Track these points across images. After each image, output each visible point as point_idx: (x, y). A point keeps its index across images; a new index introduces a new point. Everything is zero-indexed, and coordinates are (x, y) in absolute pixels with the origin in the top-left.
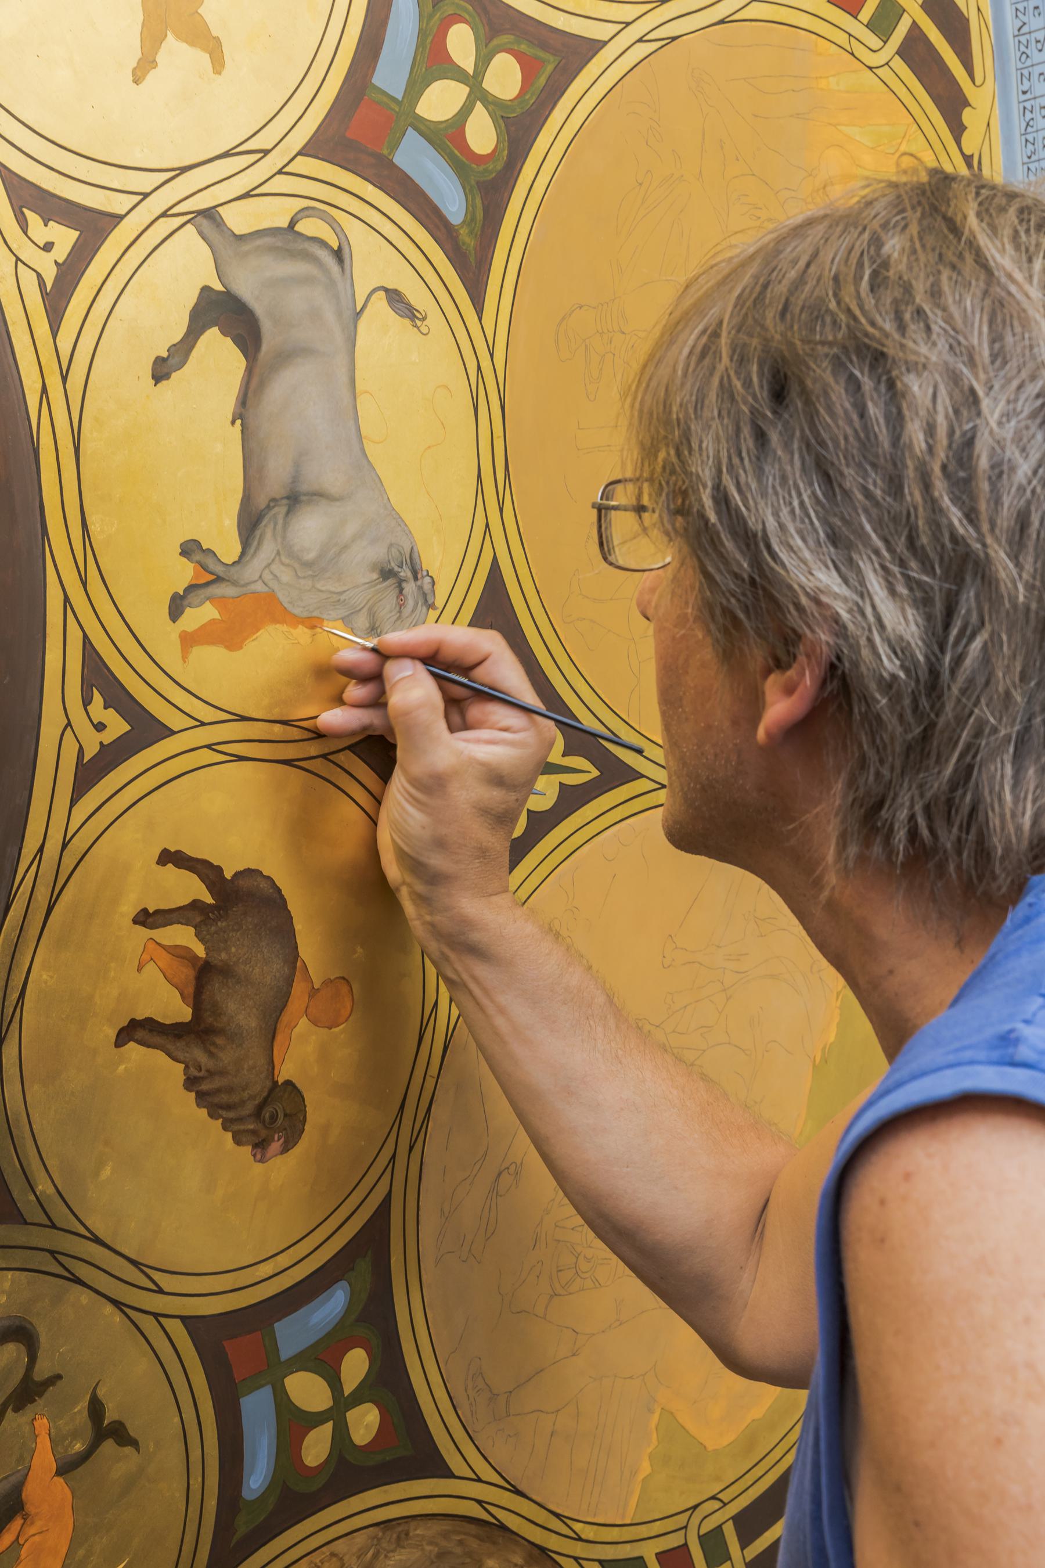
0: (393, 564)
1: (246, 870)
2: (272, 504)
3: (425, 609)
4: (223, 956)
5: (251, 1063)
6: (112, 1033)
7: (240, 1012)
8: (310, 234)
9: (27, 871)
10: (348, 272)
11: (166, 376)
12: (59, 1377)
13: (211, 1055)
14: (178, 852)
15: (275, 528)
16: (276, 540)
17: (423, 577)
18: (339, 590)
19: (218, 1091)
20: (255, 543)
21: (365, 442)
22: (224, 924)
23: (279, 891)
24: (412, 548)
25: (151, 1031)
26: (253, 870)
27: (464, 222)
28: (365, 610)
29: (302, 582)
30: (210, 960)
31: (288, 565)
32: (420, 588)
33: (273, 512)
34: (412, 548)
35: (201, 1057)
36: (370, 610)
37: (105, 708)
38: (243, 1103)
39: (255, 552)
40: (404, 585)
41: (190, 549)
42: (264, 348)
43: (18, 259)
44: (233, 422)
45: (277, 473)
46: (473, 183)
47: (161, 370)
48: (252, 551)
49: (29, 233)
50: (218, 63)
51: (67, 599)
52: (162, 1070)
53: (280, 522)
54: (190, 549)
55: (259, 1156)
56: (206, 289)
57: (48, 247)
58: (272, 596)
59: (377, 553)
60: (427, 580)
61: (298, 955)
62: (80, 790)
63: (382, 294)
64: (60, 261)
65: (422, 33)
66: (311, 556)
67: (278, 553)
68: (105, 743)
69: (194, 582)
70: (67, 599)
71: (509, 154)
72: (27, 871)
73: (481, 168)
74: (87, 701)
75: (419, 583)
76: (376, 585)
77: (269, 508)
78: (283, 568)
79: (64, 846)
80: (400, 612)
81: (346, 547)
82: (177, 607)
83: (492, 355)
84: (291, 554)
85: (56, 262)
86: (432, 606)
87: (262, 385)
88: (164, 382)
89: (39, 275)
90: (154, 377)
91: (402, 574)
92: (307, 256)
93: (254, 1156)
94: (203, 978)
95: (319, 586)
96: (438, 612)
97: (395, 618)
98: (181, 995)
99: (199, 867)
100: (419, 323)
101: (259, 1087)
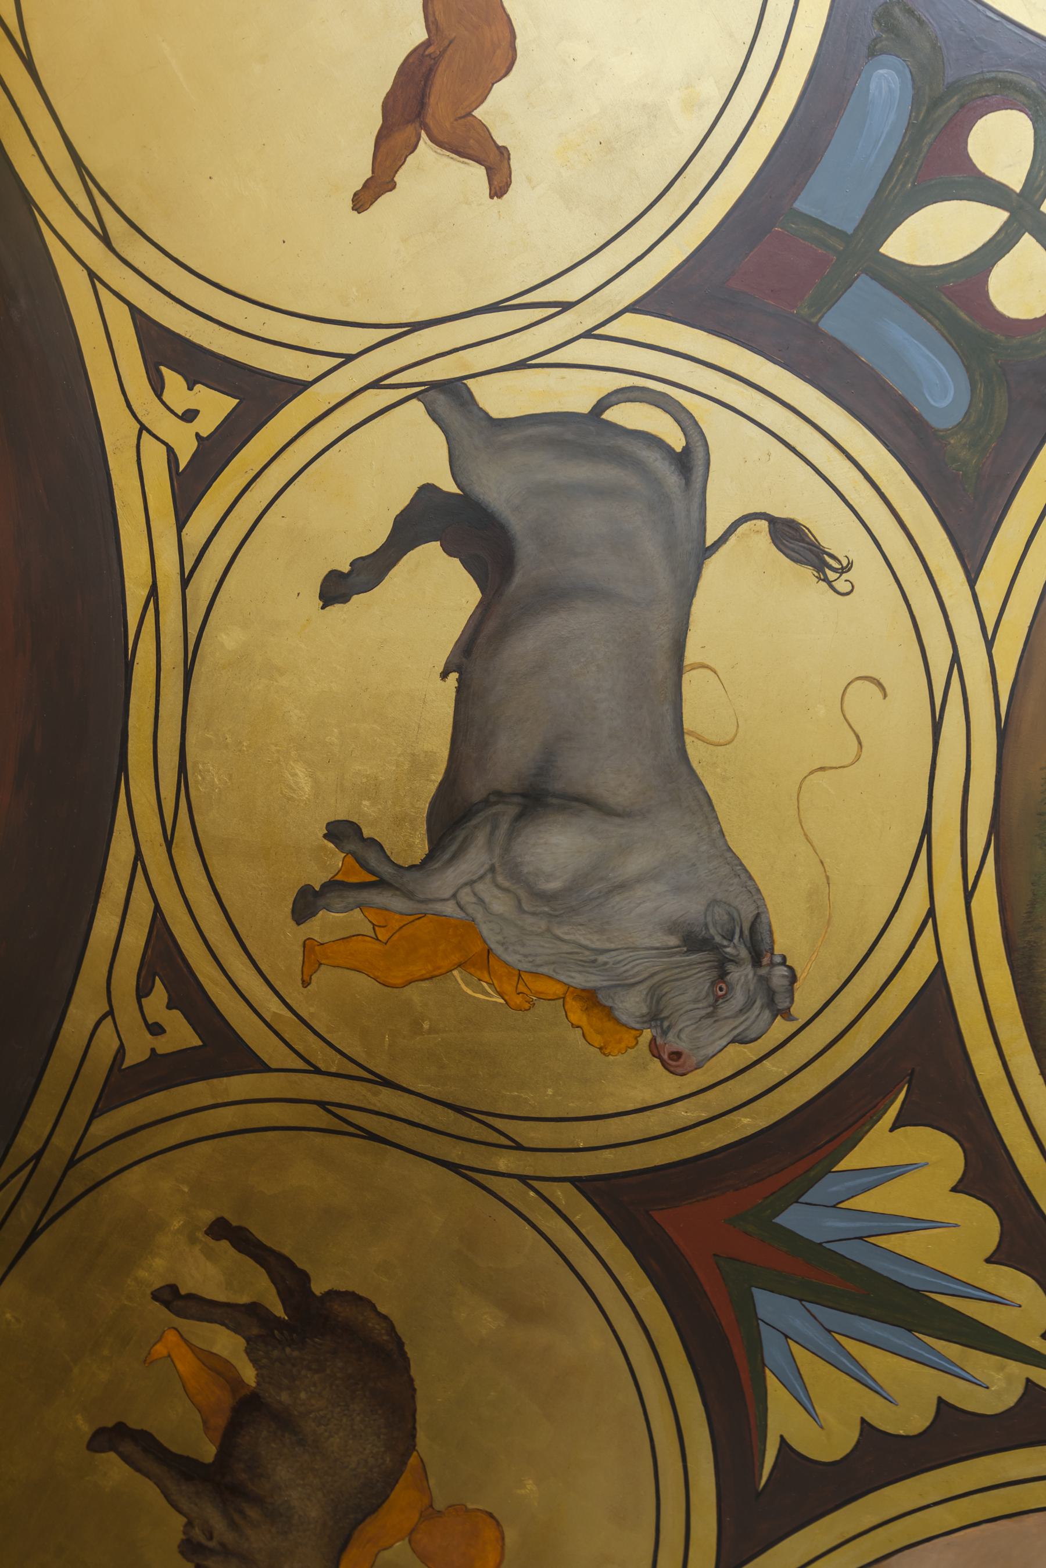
0: (712, 931)
1: (347, 1293)
2: (493, 799)
3: (767, 1014)
4: (284, 1397)
6: (86, 1429)
7: (296, 1485)
8: (630, 425)
9: (13, 1175)
10: (697, 486)
11: (345, 599)
13: (233, 1525)
14: (241, 1229)
15: (492, 833)
17: (772, 965)
18: (598, 945)
20: (454, 848)
21: (688, 739)
22: (296, 1353)
23: (400, 1344)
24: (758, 916)
26: (361, 1298)
27: (960, 426)
28: (643, 988)
32: (764, 981)
33: (494, 809)
34: (758, 916)
35: (218, 1524)
36: (653, 989)
37: (169, 1007)
40: (730, 967)
42: (517, 579)
43: (143, 428)
44: (444, 675)
45: (511, 756)
47: (336, 589)
48: (446, 856)
49: (165, 397)
51: (138, 856)
53: (504, 826)
56: (427, 491)
57: (190, 416)
58: (470, 925)
59: (690, 907)
60: (782, 971)
61: (413, 1447)
63: (764, 524)
64: (204, 434)
65: (915, 133)
66: (554, 885)
67: (492, 869)
69: (339, 878)
70: (138, 856)
72: (13, 1175)
75: (763, 971)
77: (486, 803)
78: (496, 891)
79: (72, 1163)
80: (715, 1006)
81: (623, 887)
82: (306, 903)
83: (989, 644)
84: (515, 873)
85: (197, 435)
86: (786, 1014)
87: (504, 632)
88: (337, 607)
89: (170, 450)
90: (321, 598)
91: (728, 950)
95: (558, 932)
97: (703, 1012)
98: (205, 1422)
100: (831, 575)
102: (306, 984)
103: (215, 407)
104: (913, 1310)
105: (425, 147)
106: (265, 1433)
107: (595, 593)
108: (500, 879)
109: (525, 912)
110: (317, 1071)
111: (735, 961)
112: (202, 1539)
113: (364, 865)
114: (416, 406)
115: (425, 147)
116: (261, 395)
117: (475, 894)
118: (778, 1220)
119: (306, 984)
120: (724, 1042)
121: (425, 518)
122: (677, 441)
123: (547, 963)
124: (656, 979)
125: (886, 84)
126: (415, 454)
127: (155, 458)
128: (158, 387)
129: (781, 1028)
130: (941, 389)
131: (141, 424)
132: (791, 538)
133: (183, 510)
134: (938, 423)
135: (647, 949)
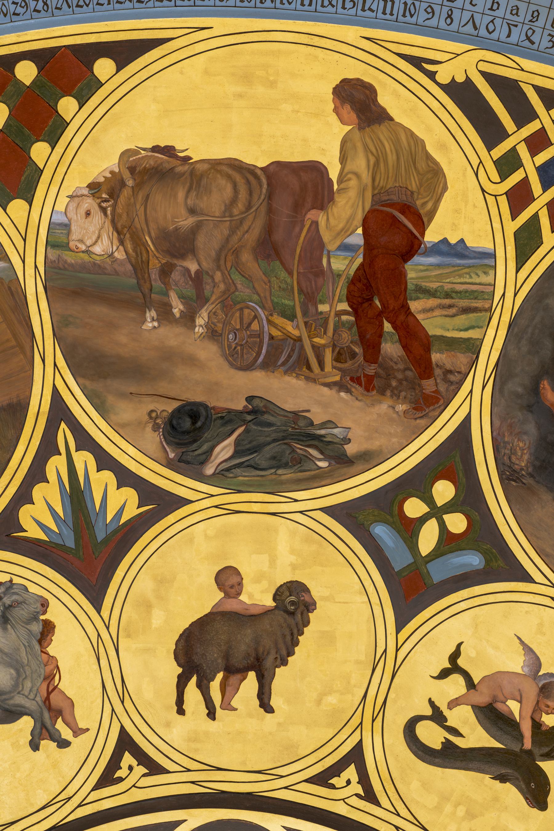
1: (176, 660)
3: (14, 587)
4: (220, 661)
5: (268, 627)
6: (269, 715)
12: (430, 700)
13: (268, 653)
15: (7, 699)
16: (13, 697)
18: (23, 648)
19: (285, 643)
20: (19, 709)
22: (204, 665)
25: (263, 694)
28: (28, 627)
29: (28, 673)
30: (223, 668)
31: (23, 685)
35: (271, 658)
36: (27, 624)
37: (121, 768)
38: (289, 626)
39: (23, 707)
40: (7, 605)
41: (35, 746)
48: (23, 709)
51: (80, 806)
52: (282, 678)
54: (35, 746)
55: (313, 607)
62: (162, 771)
66: (13, 671)
67: (19, 693)
68: (137, 763)
69: (49, 738)
70: (80, 806)
74: (121, 780)
76: (13, 624)
78: (25, 688)
80: (21, 603)
82: (63, 744)
84: (16, 685)
86: (11, 581)
93: (313, 610)
94: (234, 671)
95: (26, 662)
96: (13, 576)
97: (25, 605)
99: (180, 690)
101: (280, 616)
102: (88, 730)
104: (76, 494)
106: (235, 660)
108: (20, 689)
109: (26, 676)
110: (113, 710)
111: (4, 605)
112: (279, 660)
113: (41, 734)
117: (29, 694)
118: (74, 548)
119: (88, 730)
120: (30, 594)
123: (38, 660)
124: (23, 625)
129: (16, 580)
135: (16, 633)
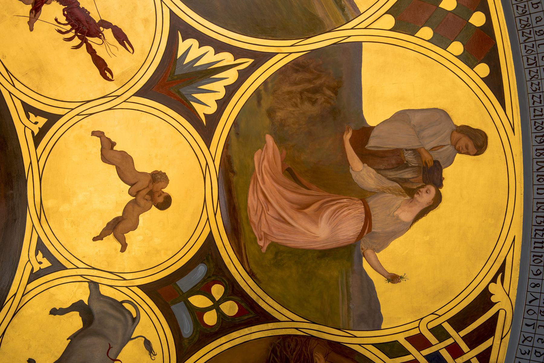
11: (55, 315)
42: (91, 327)
44: (68, 339)
46: (198, 329)
47: (54, 312)
50: (123, 250)
56: (81, 302)
63: (144, 339)
64: (42, 268)
65: (204, 280)
71: (219, 331)
73: (204, 328)
87: (84, 336)
89: (33, 268)
92: (122, 313)
100: (152, 355)
103: (46, 264)
105: (112, 235)
107: (105, 337)
114: (87, 284)
115: (112, 235)
116: (57, 266)
121: (78, 306)
122: (134, 315)
125: (201, 270)
126: (82, 294)
127: (29, 268)
128: (36, 254)
130: (187, 330)
131: (29, 259)
132: (148, 344)
133: (30, 281)
134: (184, 336)
